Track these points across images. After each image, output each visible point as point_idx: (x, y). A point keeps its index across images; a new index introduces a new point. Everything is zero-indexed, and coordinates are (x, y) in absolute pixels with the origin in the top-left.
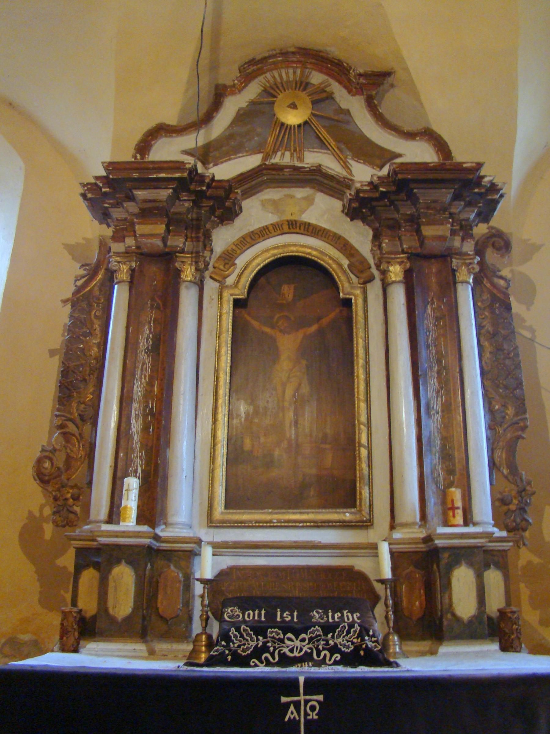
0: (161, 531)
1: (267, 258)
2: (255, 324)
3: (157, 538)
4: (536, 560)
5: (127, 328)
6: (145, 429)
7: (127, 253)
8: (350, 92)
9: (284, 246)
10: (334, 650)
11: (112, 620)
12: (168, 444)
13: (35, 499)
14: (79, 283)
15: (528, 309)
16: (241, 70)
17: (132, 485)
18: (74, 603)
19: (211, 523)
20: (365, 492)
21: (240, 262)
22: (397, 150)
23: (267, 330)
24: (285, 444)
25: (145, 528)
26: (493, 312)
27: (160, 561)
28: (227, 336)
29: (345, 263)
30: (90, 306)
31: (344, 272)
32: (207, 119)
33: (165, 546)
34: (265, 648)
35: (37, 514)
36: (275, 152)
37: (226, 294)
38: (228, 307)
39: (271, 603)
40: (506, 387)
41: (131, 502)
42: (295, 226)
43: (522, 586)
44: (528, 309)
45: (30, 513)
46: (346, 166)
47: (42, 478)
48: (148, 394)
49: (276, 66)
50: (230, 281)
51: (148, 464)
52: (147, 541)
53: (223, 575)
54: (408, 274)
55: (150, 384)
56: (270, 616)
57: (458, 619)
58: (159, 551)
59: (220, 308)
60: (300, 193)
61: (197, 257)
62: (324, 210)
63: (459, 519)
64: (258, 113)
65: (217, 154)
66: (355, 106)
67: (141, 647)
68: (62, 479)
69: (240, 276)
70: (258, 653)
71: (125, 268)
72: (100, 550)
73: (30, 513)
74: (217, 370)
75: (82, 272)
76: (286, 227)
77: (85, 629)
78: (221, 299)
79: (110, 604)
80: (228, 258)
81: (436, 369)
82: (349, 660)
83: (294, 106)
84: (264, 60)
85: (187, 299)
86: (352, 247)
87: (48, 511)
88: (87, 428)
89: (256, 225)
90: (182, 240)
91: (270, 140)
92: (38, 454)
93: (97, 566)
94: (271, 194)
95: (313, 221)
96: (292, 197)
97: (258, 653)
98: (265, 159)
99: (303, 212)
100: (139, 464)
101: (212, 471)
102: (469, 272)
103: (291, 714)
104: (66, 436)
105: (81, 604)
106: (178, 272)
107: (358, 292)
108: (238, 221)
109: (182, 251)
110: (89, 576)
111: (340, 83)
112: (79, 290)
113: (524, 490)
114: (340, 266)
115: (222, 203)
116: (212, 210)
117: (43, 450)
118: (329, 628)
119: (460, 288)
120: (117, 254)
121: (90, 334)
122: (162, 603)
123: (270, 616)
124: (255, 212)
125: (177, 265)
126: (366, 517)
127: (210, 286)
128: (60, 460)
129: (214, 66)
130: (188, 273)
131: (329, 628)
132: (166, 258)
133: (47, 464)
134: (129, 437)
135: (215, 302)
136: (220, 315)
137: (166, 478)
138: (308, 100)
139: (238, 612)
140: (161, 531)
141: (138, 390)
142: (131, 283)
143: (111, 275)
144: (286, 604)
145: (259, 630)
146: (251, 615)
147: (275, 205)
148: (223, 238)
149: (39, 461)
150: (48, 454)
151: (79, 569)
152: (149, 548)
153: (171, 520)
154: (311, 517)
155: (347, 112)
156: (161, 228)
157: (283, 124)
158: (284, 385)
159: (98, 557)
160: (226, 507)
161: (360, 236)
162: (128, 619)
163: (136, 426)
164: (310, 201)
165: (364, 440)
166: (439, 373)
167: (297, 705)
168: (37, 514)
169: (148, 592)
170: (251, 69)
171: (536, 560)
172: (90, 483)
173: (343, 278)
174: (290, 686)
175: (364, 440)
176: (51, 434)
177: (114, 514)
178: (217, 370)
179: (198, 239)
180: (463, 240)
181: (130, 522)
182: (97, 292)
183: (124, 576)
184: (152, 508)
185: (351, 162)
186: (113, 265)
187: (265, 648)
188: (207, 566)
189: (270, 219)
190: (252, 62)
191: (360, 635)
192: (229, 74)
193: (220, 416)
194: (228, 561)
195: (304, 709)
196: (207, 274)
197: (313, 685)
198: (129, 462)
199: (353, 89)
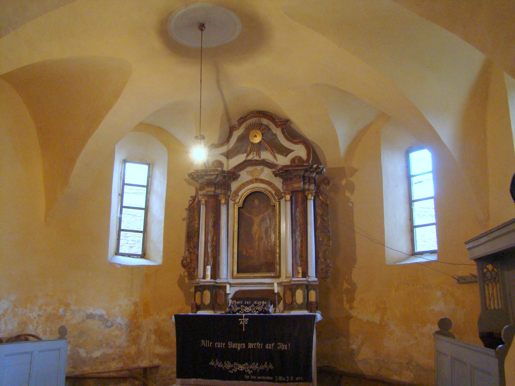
0: (217, 281)
1: (248, 192)
2: (245, 213)
3: (216, 283)
4: (349, 287)
5: (206, 219)
6: (212, 251)
7: (204, 195)
8: (276, 126)
9: (254, 188)
10: (257, 310)
11: (205, 305)
12: (219, 255)
13: (182, 271)
14: (190, 203)
15: (352, 195)
16: (238, 121)
17: (209, 268)
18: (195, 301)
19: (233, 277)
20: (278, 267)
21: (240, 194)
22: (292, 148)
23: (250, 215)
24: (256, 252)
25: (212, 280)
26: (322, 207)
27: (217, 289)
28: (236, 220)
29: (274, 192)
30: (194, 210)
31: (273, 196)
32: (228, 140)
33: (219, 285)
34: (240, 310)
35: (183, 275)
36: (250, 153)
37: (236, 206)
38: (236, 210)
39: (244, 300)
40: (324, 233)
41: (209, 273)
42: (257, 180)
43: (344, 295)
44: (352, 195)
45: (181, 275)
46: (275, 157)
47: (184, 266)
48: (213, 240)
49: (250, 118)
50: (237, 201)
51: (214, 261)
52: (213, 284)
53: (237, 293)
54: (291, 198)
55: (213, 237)
56: (243, 302)
57: (297, 304)
58: (218, 286)
59: (234, 210)
60: (259, 168)
61: (225, 194)
62: (266, 174)
63: (300, 276)
64: (244, 138)
65: (231, 155)
66: (278, 132)
67: (213, 312)
68: (189, 265)
69: (240, 200)
70: (238, 311)
71: (203, 200)
72: (201, 286)
73: (181, 275)
74: (234, 231)
75: (190, 199)
76: (254, 181)
77: (198, 308)
78: (234, 207)
79: (204, 301)
80: (236, 193)
81: (299, 229)
82: (260, 312)
83: (255, 136)
84: (245, 117)
85: (223, 209)
86: (276, 187)
87: (186, 274)
88: (196, 250)
89: (245, 181)
90: (220, 190)
91: (249, 149)
92: (182, 259)
93: (200, 291)
94: (249, 169)
95: (263, 178)
96: (256, 169)
97: (238, 311)
98: (248, 156)
99: (260, 174)
100: (211, 261)
101: (233, 262)
102: (312, 196)
103: (241, 323)
104: (190, 253)
105: (197, 301)
106: (220, 201)
107: (277, 203)
108: (239, 179)
109: (221, 194)
110: (198, 294)
111: (273, 123)
112: (190, 205)
113: (328, 266)
114: (272, 194)
115: (233, 175)
116: (229, 179)
117: (183, 257)
118: (256, 305)
119: (308, 201)
120: (201, 195)
121: (195, 220)
122: (218, 301)
123: (243, 302)
124: (244, 176)
125: (219, 198)
126: (278, 274)
127: (231, 203)
128: (189, 260)
129: (229, 120)
130: (223, 201)
131: (256, 305)
132: (216, 197)
133: (185, 262)
134: (208, 253)
135: (233, 208)
136: (234, 212)
137: (219, 265)
138: (260, 133)
139: (235, 301)
140: (217, 281)
141: (210, 239)
142: (206, 205)
143: (199, 202)
144: (248, 299)
145: (239, 306)
146: (238, 302)
147: (251, 173)
148: (234, 186)
149: (182, 261)
150: (185, 259)
151: (196, 292)
152: (214, 286)
153: (221, 277)
154: (262, 275)
155: (275, 135)
156: (213, 189)
157: (252, 143)
158: (255, 234)
159: (201, 288)
160: (237, 273)
161: (278, 183)
162: (209, 305)
163: (210, 250)
164: (262, 170)
165: (278, 251)
166: (300, 230)
167: (243, 321)
168: (183, 275)
169: (214, 297)
170: (242, 120)
171: (349, 287)
172: (198, 267)
173: (273, 198)
174: (241, 317)
175: (278, 251)
176: (185, 253)
177: (204, 277)
178: (234, 231)
179: (225, 189)
180: (309, 185)
181: (208, 279)
182: (196, 206)
183: (207, 294)
184: (215, 274)
185: (277, 155)
186: (200, 199)
187: (240, 310)
188: (230, 291)
189: (249, 178)
190: (241, 118)
191: (264, 307)
192: (235, 122)
193: (235, 245)
194: (238, 289)
195: (244, 322)
196: (230, 198)
197: (246, 317)
198: (208, 261)
199: (277, 126)
